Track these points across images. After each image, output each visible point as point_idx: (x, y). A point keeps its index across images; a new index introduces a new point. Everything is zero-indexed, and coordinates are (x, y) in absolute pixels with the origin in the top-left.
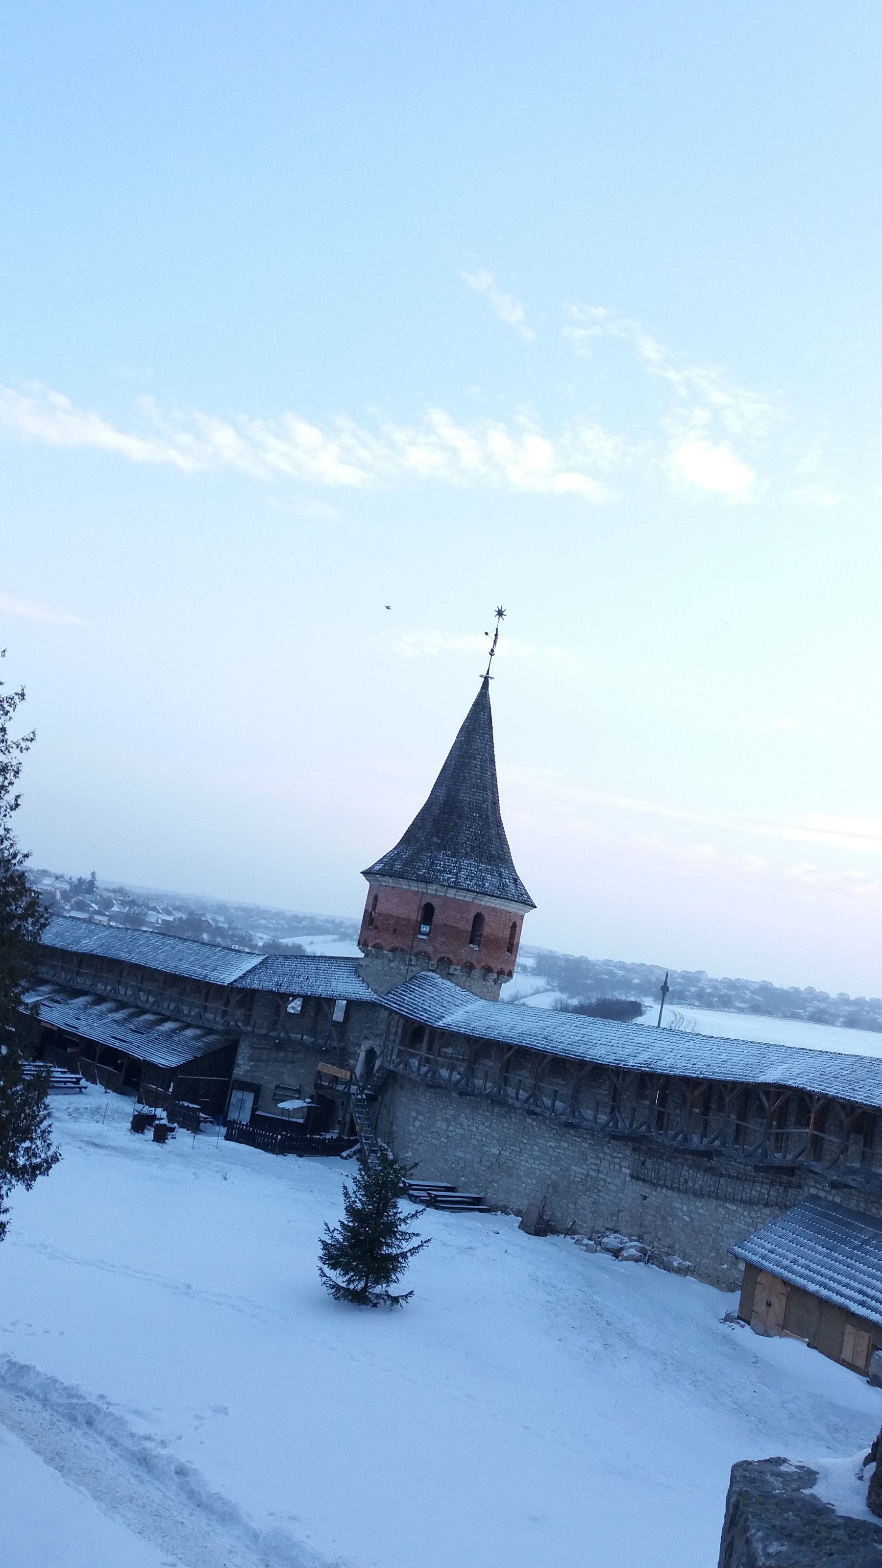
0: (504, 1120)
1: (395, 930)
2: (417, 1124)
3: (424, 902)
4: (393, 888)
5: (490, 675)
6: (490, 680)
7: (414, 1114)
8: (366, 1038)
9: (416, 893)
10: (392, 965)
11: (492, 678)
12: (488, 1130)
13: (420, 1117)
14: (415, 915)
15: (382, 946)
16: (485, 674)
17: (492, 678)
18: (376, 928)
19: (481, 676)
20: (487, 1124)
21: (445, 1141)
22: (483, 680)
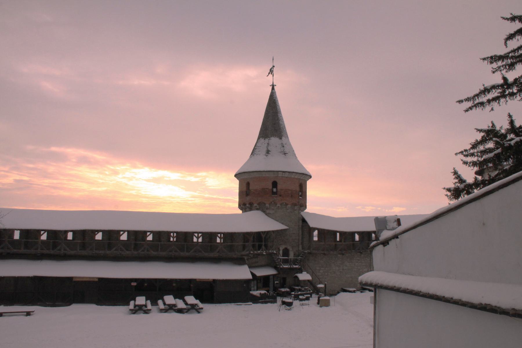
0: (367, 258)
1: (292, 196)
2: (321, 271)
3: (300, 182)
4: (287, 177)
5: (274, 84)
6: (275, 87)
7: (318, 268)
8: (281, 245)
9: (297, 179)
10: (288, 211)
11: (275, 85)
12: (360, 264)
13: (322, 269)
14: (298, 189)
15: (252, 203)
16: (272, 84)
17: (275, 85)
18: (280, 196)
19: (271, 86)
20: (359, 262)
21: (339, 273)
22: (271, 87)
